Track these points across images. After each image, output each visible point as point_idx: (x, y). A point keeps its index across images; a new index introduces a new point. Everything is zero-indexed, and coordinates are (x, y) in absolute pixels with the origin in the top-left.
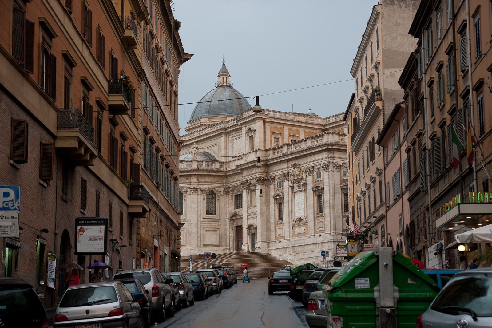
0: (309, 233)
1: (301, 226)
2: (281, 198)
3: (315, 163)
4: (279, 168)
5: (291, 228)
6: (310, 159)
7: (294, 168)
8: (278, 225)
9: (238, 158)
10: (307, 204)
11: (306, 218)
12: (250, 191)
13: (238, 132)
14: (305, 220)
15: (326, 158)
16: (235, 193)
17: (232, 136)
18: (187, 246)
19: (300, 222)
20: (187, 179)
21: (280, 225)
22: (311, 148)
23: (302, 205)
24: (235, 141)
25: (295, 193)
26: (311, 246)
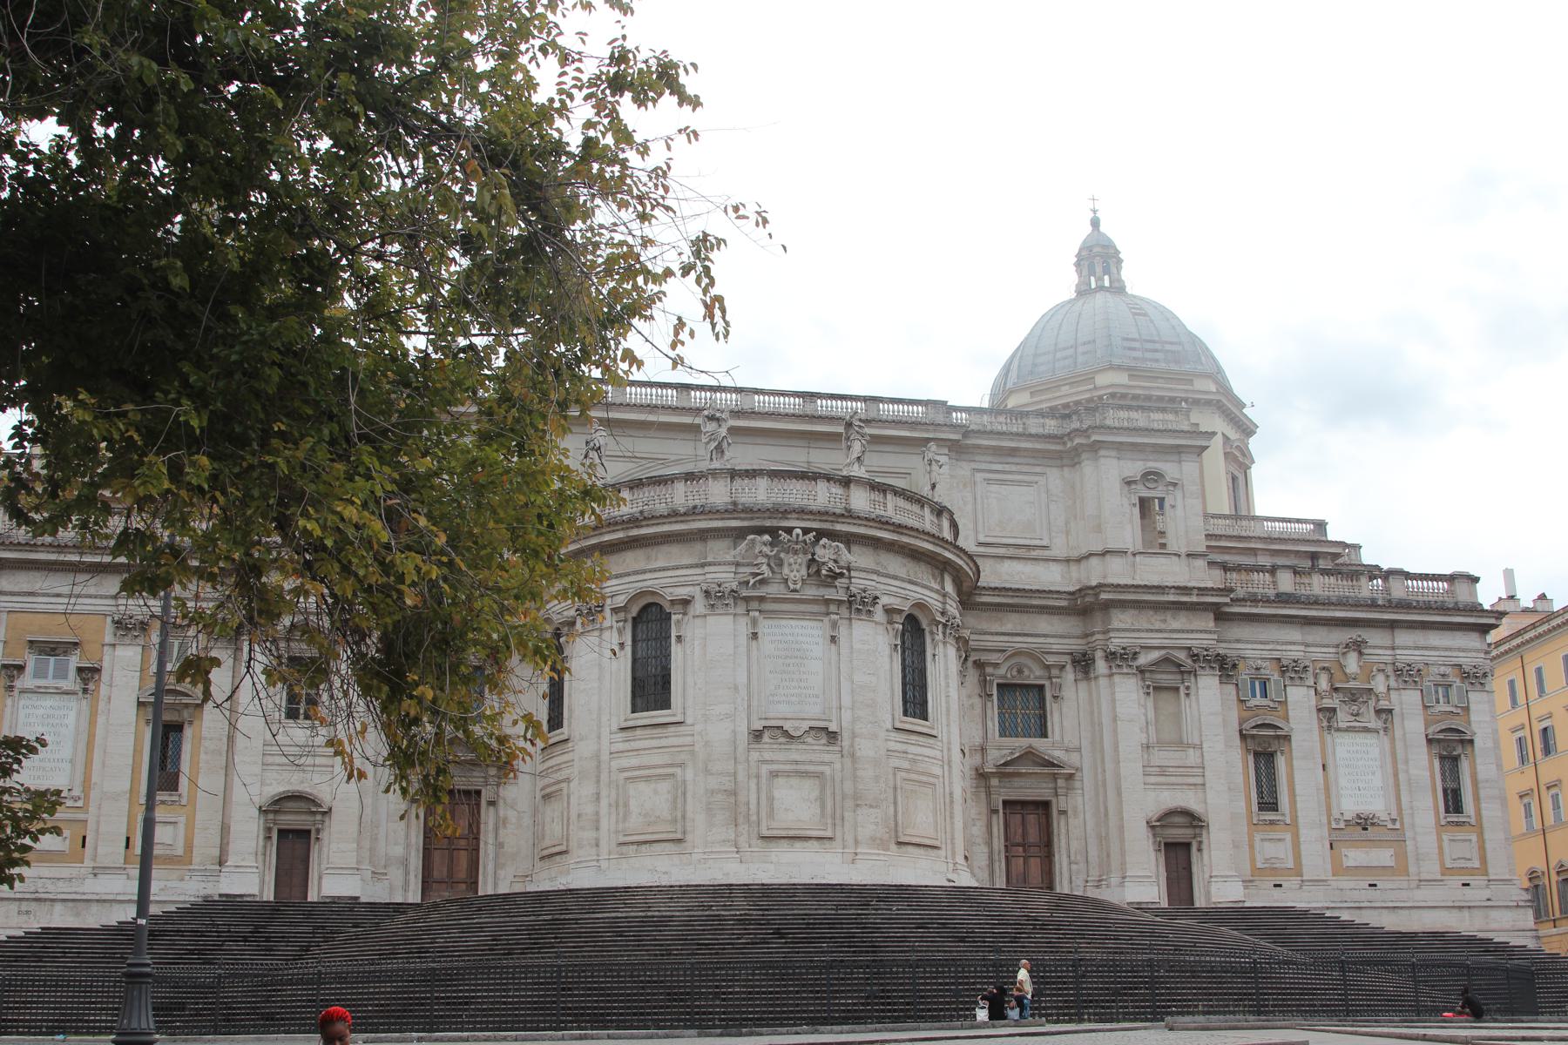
0: (1412, 869)
2: (1278, 737)
6: (1403, 638)
7: (1344, 654)
8: (1260, 827)
9: (1011, 552)
10: (1396, 775)
11: (1394, 821)
12: (1151, 690)
13: (1010, 460)
15: (1478, 651)
16: (1002, 677)
18: (942, 853)
19: (1365, 829)
21: (1267, 828)
24: (994, 488)
25: (1336, 734)
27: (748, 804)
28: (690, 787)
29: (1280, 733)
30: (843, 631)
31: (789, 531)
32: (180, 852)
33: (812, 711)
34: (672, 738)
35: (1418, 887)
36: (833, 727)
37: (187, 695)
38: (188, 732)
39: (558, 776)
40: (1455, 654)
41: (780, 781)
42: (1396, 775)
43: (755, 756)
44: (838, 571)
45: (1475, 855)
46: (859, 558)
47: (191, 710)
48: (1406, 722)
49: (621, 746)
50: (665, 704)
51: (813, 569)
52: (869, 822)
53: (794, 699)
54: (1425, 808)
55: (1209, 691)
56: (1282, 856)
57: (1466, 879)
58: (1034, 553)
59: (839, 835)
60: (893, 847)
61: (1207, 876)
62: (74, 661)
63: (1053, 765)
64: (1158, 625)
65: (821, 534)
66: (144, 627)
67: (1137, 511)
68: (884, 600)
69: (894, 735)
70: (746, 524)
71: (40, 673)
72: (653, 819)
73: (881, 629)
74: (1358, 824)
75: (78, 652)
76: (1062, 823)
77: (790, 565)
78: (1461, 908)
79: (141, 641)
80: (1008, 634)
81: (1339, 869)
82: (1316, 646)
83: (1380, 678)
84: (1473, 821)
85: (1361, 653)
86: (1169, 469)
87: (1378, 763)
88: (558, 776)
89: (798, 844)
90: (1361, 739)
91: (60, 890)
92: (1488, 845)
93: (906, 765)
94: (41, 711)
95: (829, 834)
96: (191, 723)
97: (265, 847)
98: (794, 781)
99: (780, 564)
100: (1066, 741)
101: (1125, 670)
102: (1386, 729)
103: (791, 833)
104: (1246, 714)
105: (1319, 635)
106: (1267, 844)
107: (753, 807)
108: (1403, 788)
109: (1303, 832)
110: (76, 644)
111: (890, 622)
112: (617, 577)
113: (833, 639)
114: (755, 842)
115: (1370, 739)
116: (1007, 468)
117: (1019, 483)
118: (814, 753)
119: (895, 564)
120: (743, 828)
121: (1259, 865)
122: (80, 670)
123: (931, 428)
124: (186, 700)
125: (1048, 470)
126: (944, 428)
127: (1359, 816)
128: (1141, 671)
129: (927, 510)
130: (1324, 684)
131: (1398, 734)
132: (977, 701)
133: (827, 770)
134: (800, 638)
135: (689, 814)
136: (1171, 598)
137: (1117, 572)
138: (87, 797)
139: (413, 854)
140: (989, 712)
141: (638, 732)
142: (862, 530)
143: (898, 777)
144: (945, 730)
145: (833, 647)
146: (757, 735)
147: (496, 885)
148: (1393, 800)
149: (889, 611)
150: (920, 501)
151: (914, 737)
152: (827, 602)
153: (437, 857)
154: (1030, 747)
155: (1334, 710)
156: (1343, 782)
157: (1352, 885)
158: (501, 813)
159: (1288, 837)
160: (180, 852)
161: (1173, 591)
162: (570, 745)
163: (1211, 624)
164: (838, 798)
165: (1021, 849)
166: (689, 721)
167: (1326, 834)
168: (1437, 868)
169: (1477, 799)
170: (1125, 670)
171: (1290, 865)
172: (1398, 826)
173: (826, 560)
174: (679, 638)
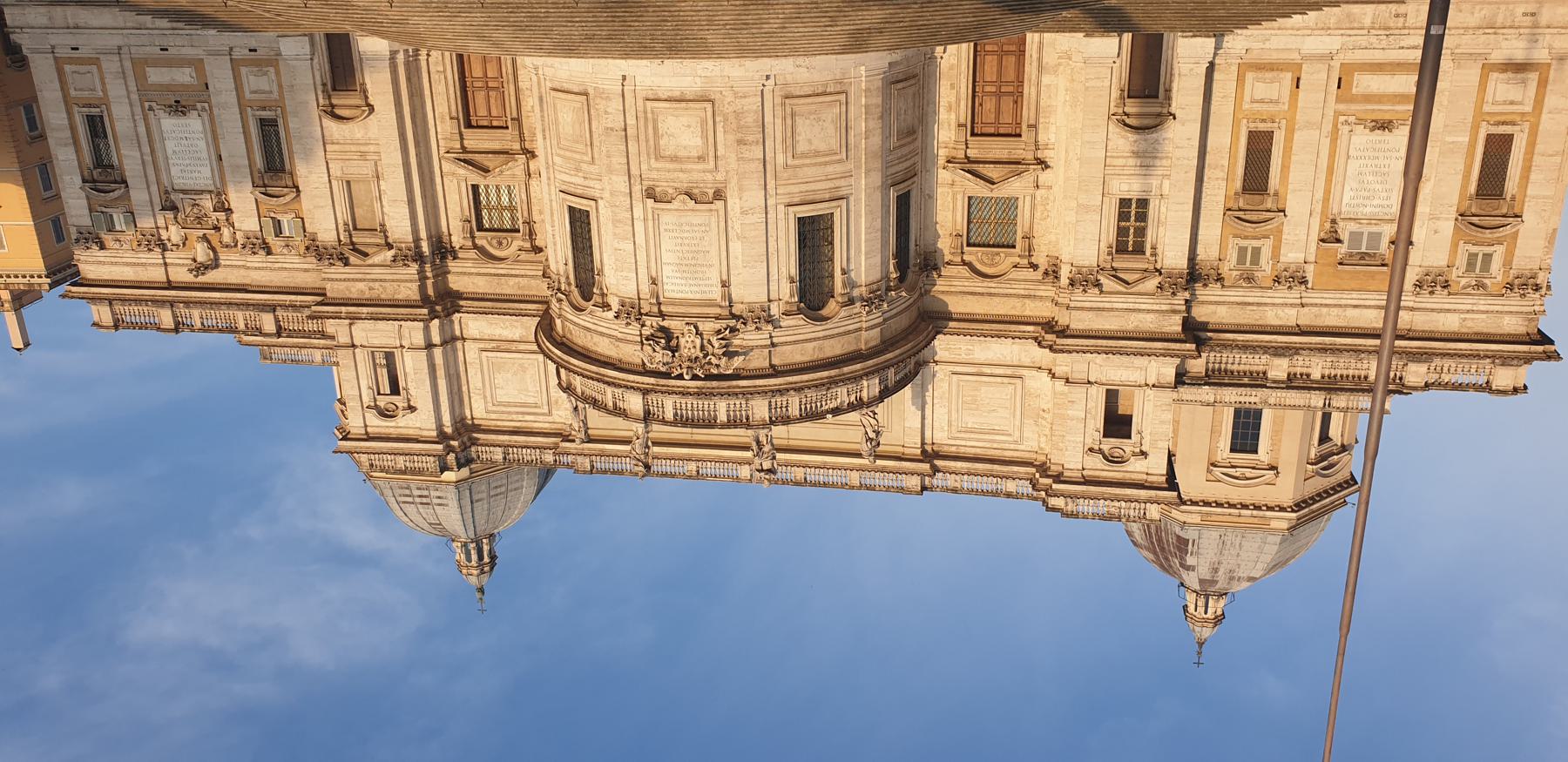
0: (128, 64)
1: (168, 88)
3: (129, 257)
4: (285, 274)
5: (209, 87)
6: (158, 275)
8: (274, 104)
9: (513, 346)
10: (153, 151)
11: (151, 109)
13: (518, 424)
14: (154, 104)
17: (550, 419)
18: (549, 85)
19: (176, 102)
20: (571, 334)
22: (157, 302)
23: (177, 149)
24: (531, 400)
26: (95, 23)
27: (725, 131)
28: (779, 147)
29: (263, 189)
30: (645, 289)
31: (695, 377)
32: (1250, 76)
33: (669, 217)
34: (796, 191)
35: (120, 48)
36: (650, 202)
37: (1238, 218)
38: (1238, 184)
39: (899, 153)
40: (108, 259)
41: (695, 154)
42: (153, 151)
43: (720, 177)
44: (651, 342)
45: (69, 79)
46: (632, 353)
47: (1236, 207)
48: (148, 198)
49: (842, 182)
50: (802, 222)
51: (674, 343)
52: (610, 114)
53: (687, 228)
54: (121, 118)
55: (326, 230)
56: (251, 78)
57: (75, 54)
58: (493, 344)
59: (640, 103)
60: (591, 91)
61: (316, 61)
62: (1343, 249)
63: (465, 161)
64: (377, 285)
65: (667, 375)
66: (1277, 280)
67: (402, 384)
68: (611, 314)
69: (597, 195)
70: (734, 383)
71: (1375, 238)
72: (812, 117)
73: (613, 289)
74: (184, 107)
75: (1339, 256)
76: (453, 108)
77: (695, 347)
78: (77, 27)
79: (1280, 266)
80: (512, 276)
81: (197, 64)
82: (237, 268)
83: (176, 239)
84: (76, 109)
85: (195, 260)
86: (376, 424)
87: (171, 162)
88: (899, 153)
89: (677, 94)
90: (189, 183)
91: (1365, 38)
92: (57, 85)
93: (584, 166)
94: (1375, 202)
95: (649, 104)
96: (1236, 194)
97: (1171, 82)
98: (682, 153)
99: (702, 348)
100: (455, 181)
101: (403, 245)
102: (167, 192)
103: (683, 105)
104: (295, 206)
105: (234, 277)
106: (267, 88)
107: (720, 129)
108: (144, 139)
109: (232, 98)
110: (1340, 264)
111: (603, 295)
112: (849, 332)
113: (654, 283)
114: (717, 97)
115: (179, 183)
116: (520, 417)
117: (509, 404)
118: (666, 177)
119: (603, 347)
120: (729, 109)
121: (272, 70)
122: (1338, 241)
123: (586, 452)
124: (1241, 214)
125: (485, 416)
126: (574, 452)
127: (184, 114)
128: (390, 246)
129: (579, 391)
130: (226, 232)
131: (154, 188)
132: (536, 218)
133: (653, 161)
134: (683, 282)
135: (779, 121)
136: (365, 310)
137: (414, 333)
138: (1335, 126)
139: (1034, 77)
140: (525, 207)
141: (827, 196)
142: (632, 377)
143: (590, 155)
144: (553, 197)
145: (654, 275)
146: (719, 195)
147: (959, 51)
148: (154, 128)
149: (606, 306)
150: (586, 399)
151: (579, 192)
152: (662, 315)
153: (1010, 75)
154: (485, 177)
155: (215, 211)
156: (202, 144)
157: (184, 51)
158: (953, 116)
159: (248, 95)
160: (1250, 76)
161: (364, 316)
162: (890, 181)
163: (328, 286)
164: (642, 137)
165: (490, 85)
166: (781, 208)
167: (214, 100)
168: (104, 65)
169: (73, 128)
170: (403, 245)
171: (244, 70)
172: (147, 104)
173: (661, 352)
174: (792, 281)
